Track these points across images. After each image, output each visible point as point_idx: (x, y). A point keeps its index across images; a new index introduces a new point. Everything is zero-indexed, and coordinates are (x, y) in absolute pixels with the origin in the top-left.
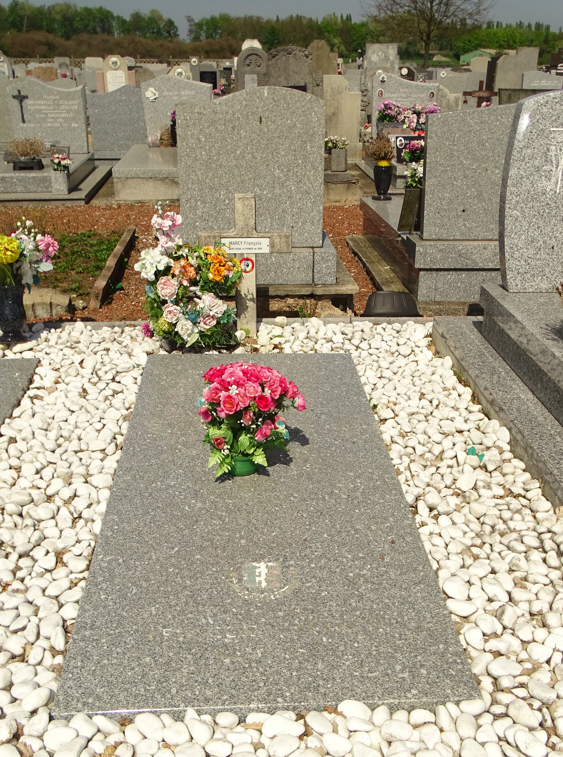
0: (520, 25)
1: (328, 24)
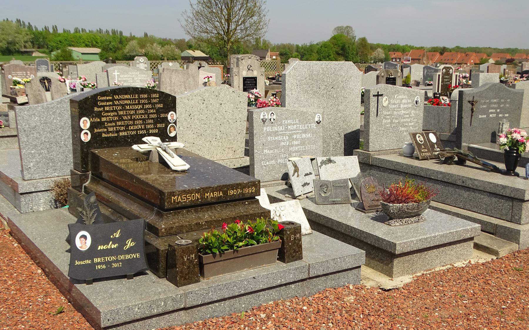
0: (100, 31)
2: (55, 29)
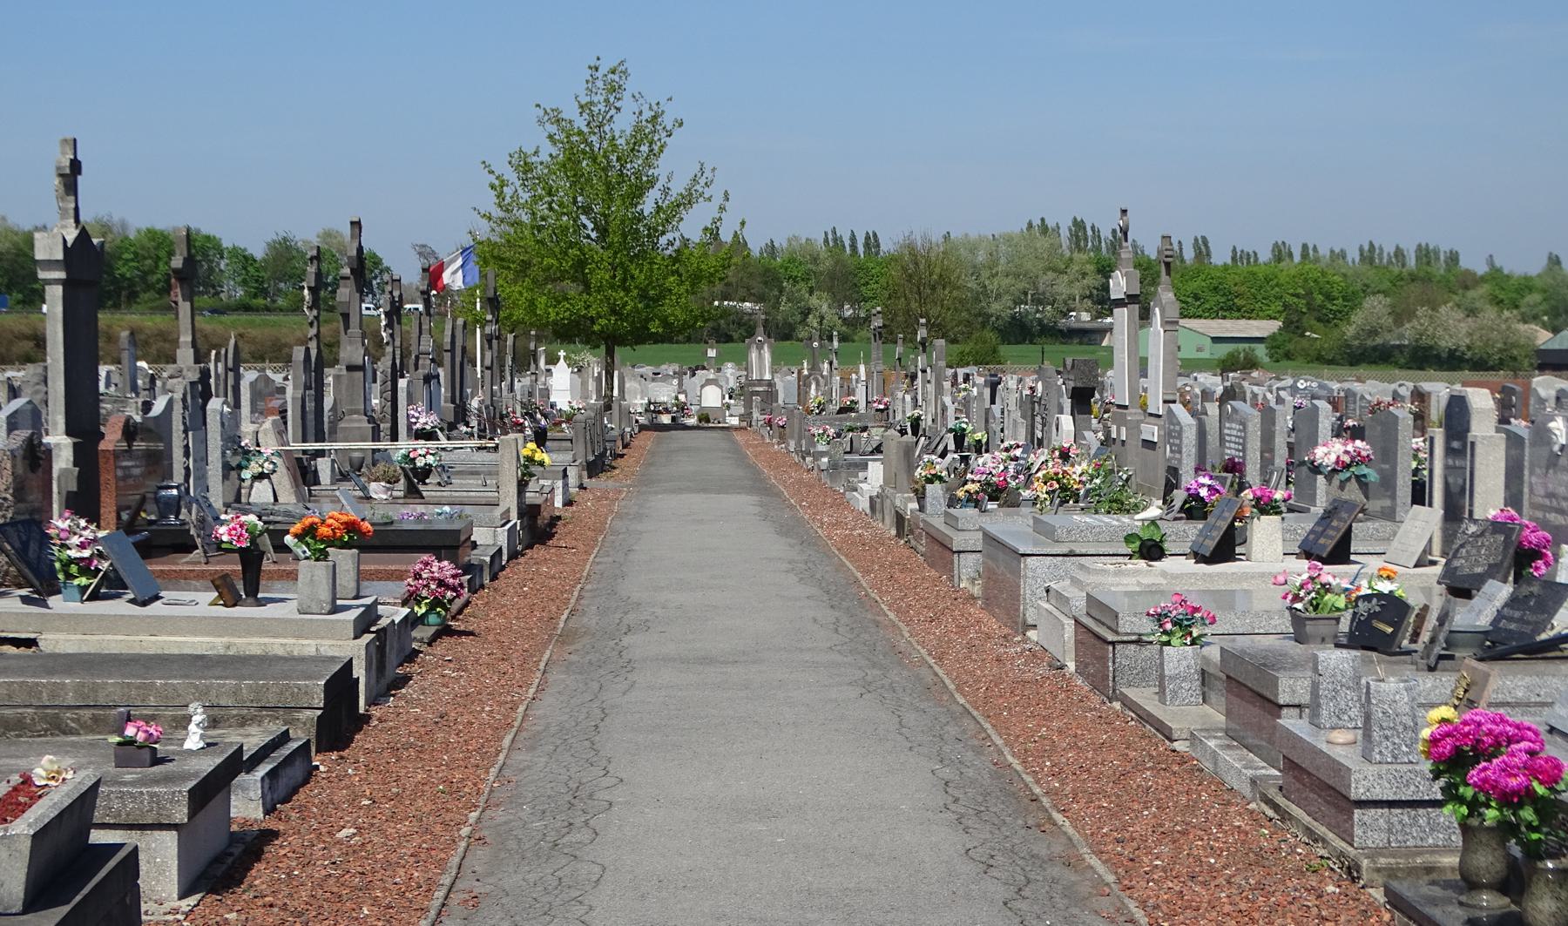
1: (792, 260)
2: (1202, 248)
